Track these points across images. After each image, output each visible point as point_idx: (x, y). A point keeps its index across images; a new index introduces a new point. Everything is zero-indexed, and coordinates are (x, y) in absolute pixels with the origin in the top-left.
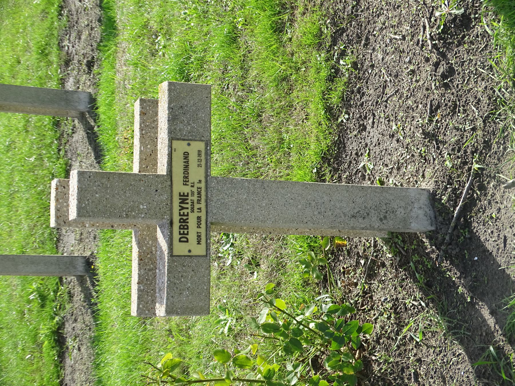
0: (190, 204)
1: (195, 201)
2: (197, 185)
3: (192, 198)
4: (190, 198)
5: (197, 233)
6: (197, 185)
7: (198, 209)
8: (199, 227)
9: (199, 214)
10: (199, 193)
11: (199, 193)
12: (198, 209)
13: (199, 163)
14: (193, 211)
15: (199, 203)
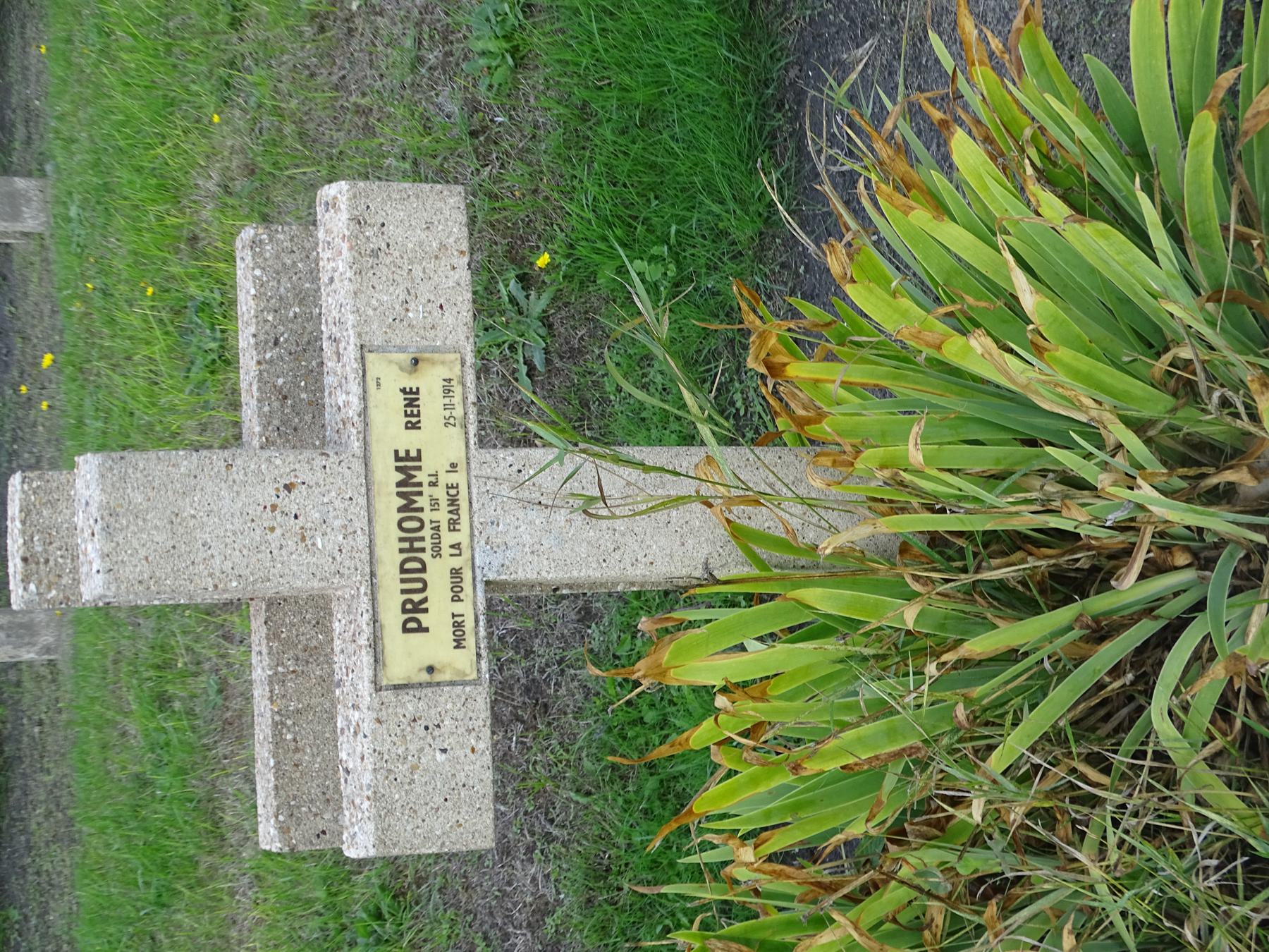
0: (427, 532)
1: (444, 526)
2: (445, 479)
3: (435, 516)
4: (426, 516)
5: (454, 616)
6: (445, 479)
7: (452, 547)
8: (456, 599)
9: (456, 563)
10: (453, 501)
11: (453, 501)
12: (452, 547)
13: (447, 413)
14: (437, 553)
15: (454, 530)
